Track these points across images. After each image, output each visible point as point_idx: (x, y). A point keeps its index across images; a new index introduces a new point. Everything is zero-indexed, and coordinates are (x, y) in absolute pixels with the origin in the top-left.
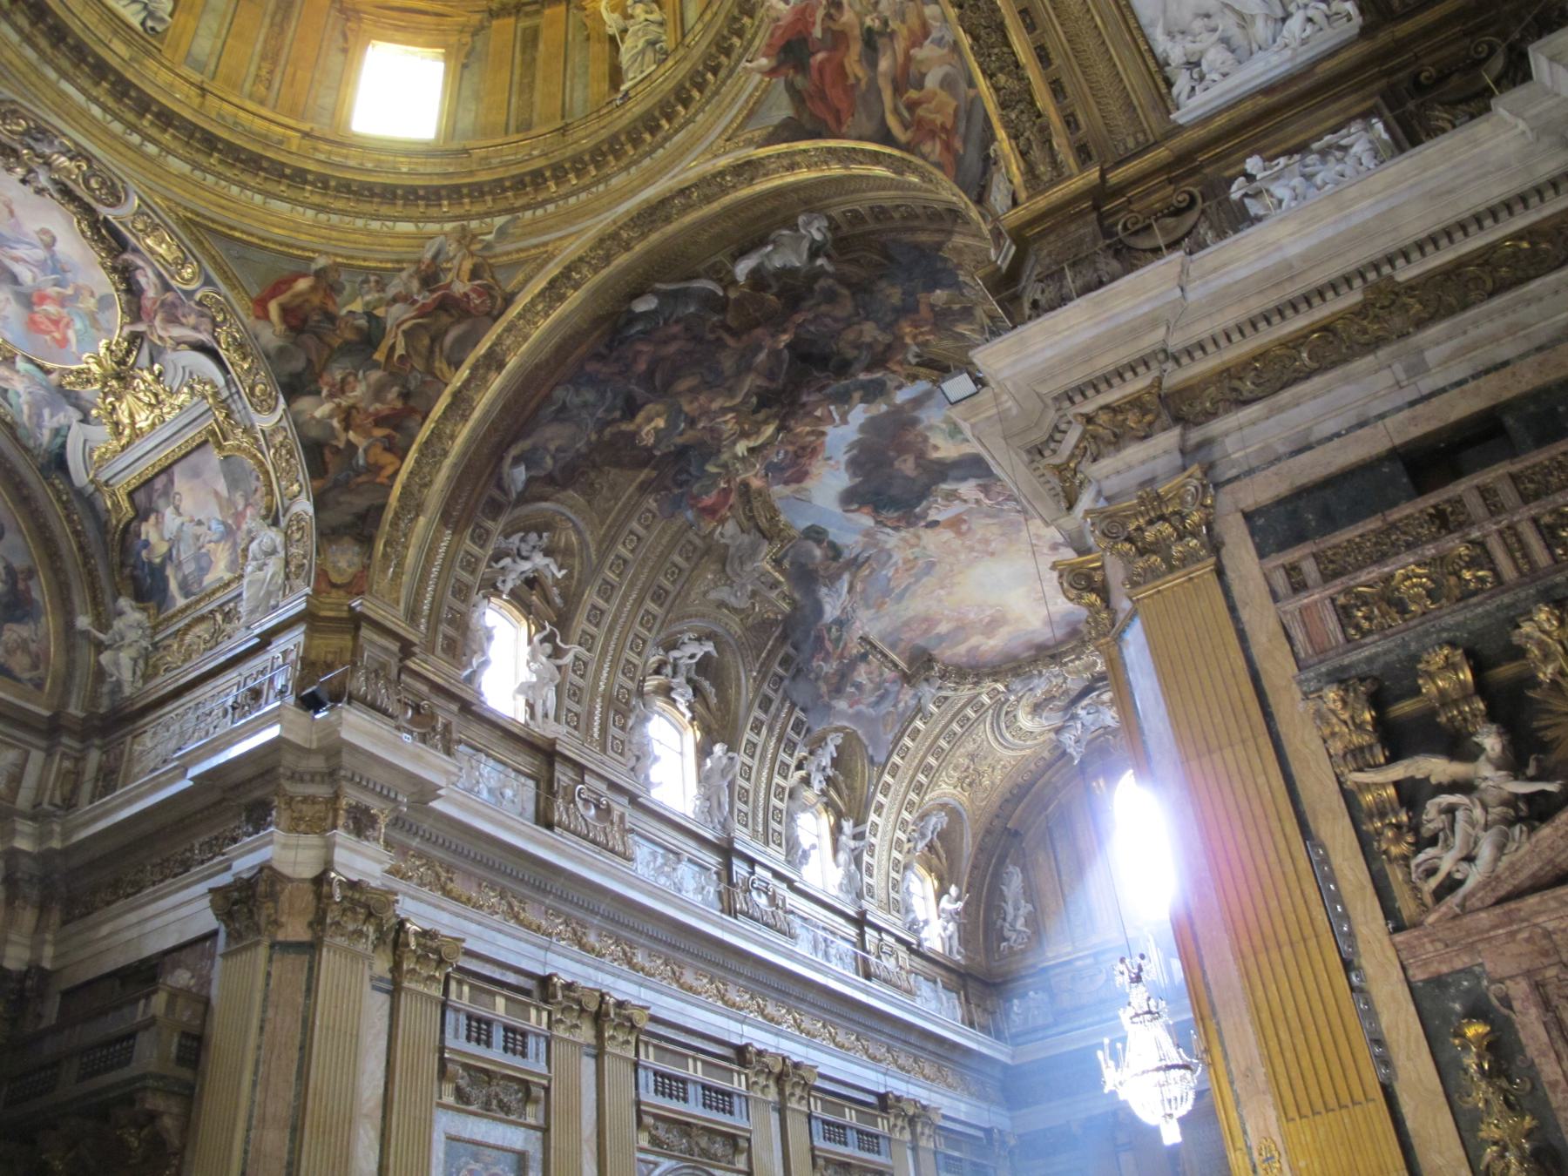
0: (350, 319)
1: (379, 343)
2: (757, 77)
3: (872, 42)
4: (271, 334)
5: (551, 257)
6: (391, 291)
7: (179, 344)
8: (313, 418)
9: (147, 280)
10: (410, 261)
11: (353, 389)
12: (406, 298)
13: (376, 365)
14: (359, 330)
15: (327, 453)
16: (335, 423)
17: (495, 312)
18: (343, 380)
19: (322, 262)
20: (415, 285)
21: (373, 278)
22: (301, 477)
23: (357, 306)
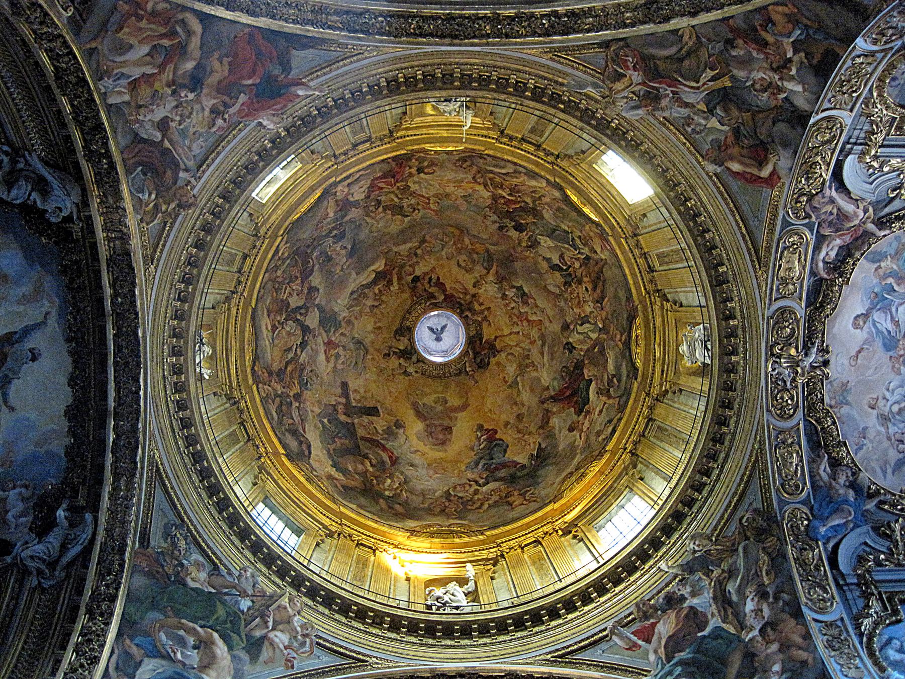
0: (726, 121)
1: (719, 90)
2: (311, 84)
3: (195, 82)
4: (780, 161)
5: (552, 50)
6: (685, 112)
7: (857, 200)
8: (805, 90)
9: (830, 251)
10: (656, 118)
11: (762, 79)
12: (677, 99)
13: (733, 78)
14: (726, 110)
15: (815, 61)
16: (794, 72)
17: (621, 43)
18: (765, 90)
19: (711, 168)
20: (664, 102)
21: (689, 130)
22: (849, 63)
23: (714, 123)
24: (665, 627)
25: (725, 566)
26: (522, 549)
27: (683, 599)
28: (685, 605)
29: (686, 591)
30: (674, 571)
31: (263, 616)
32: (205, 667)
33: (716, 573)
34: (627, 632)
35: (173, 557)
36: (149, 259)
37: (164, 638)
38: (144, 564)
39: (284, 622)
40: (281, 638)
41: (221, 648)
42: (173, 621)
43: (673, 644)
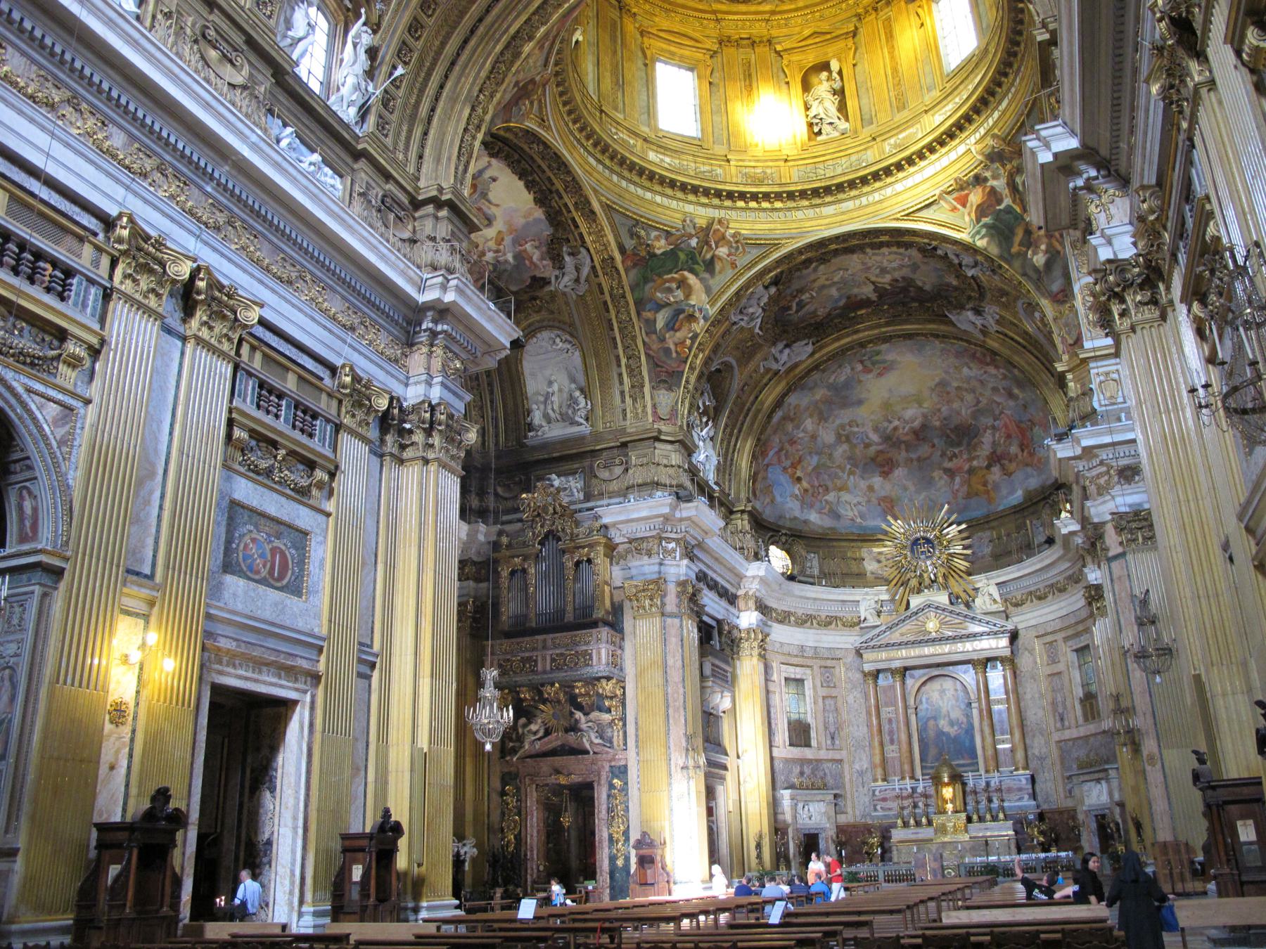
24: (976, 197)
25: (1015, 163)
26: (876, 9)
27: (986, 180)
28: (989, 184)
29: (988, 174)
30: (980, 158)
31: (707, 243)
32: (688, 296)
33: (1009, 167)
34: (949, 198)
35: (641, 244)
36: (542, 121)
37: (659, 295)
38: (629, 263)
39: (722, 239)
40: (723, 251)
41: (692, 279)
42: (659, 281)
43: (981, 211)
